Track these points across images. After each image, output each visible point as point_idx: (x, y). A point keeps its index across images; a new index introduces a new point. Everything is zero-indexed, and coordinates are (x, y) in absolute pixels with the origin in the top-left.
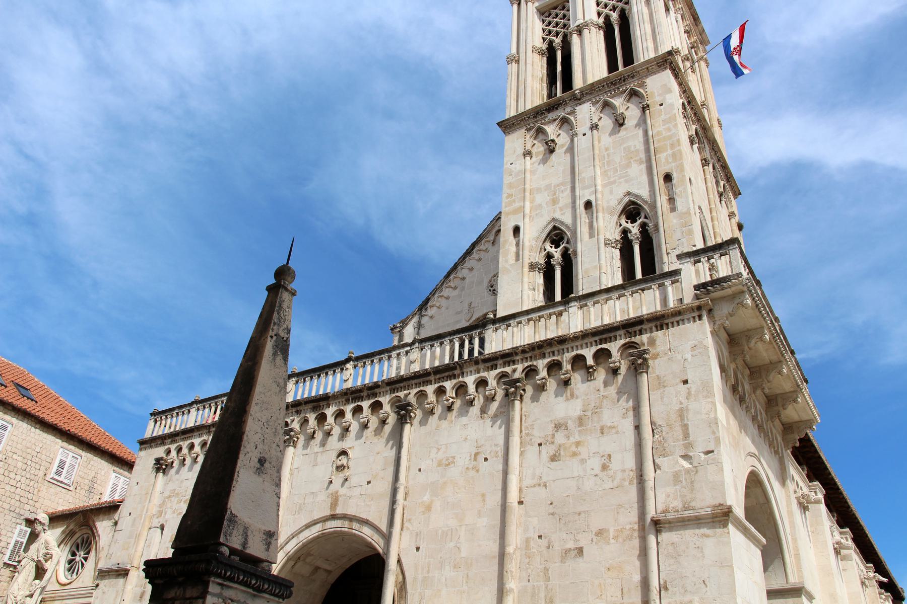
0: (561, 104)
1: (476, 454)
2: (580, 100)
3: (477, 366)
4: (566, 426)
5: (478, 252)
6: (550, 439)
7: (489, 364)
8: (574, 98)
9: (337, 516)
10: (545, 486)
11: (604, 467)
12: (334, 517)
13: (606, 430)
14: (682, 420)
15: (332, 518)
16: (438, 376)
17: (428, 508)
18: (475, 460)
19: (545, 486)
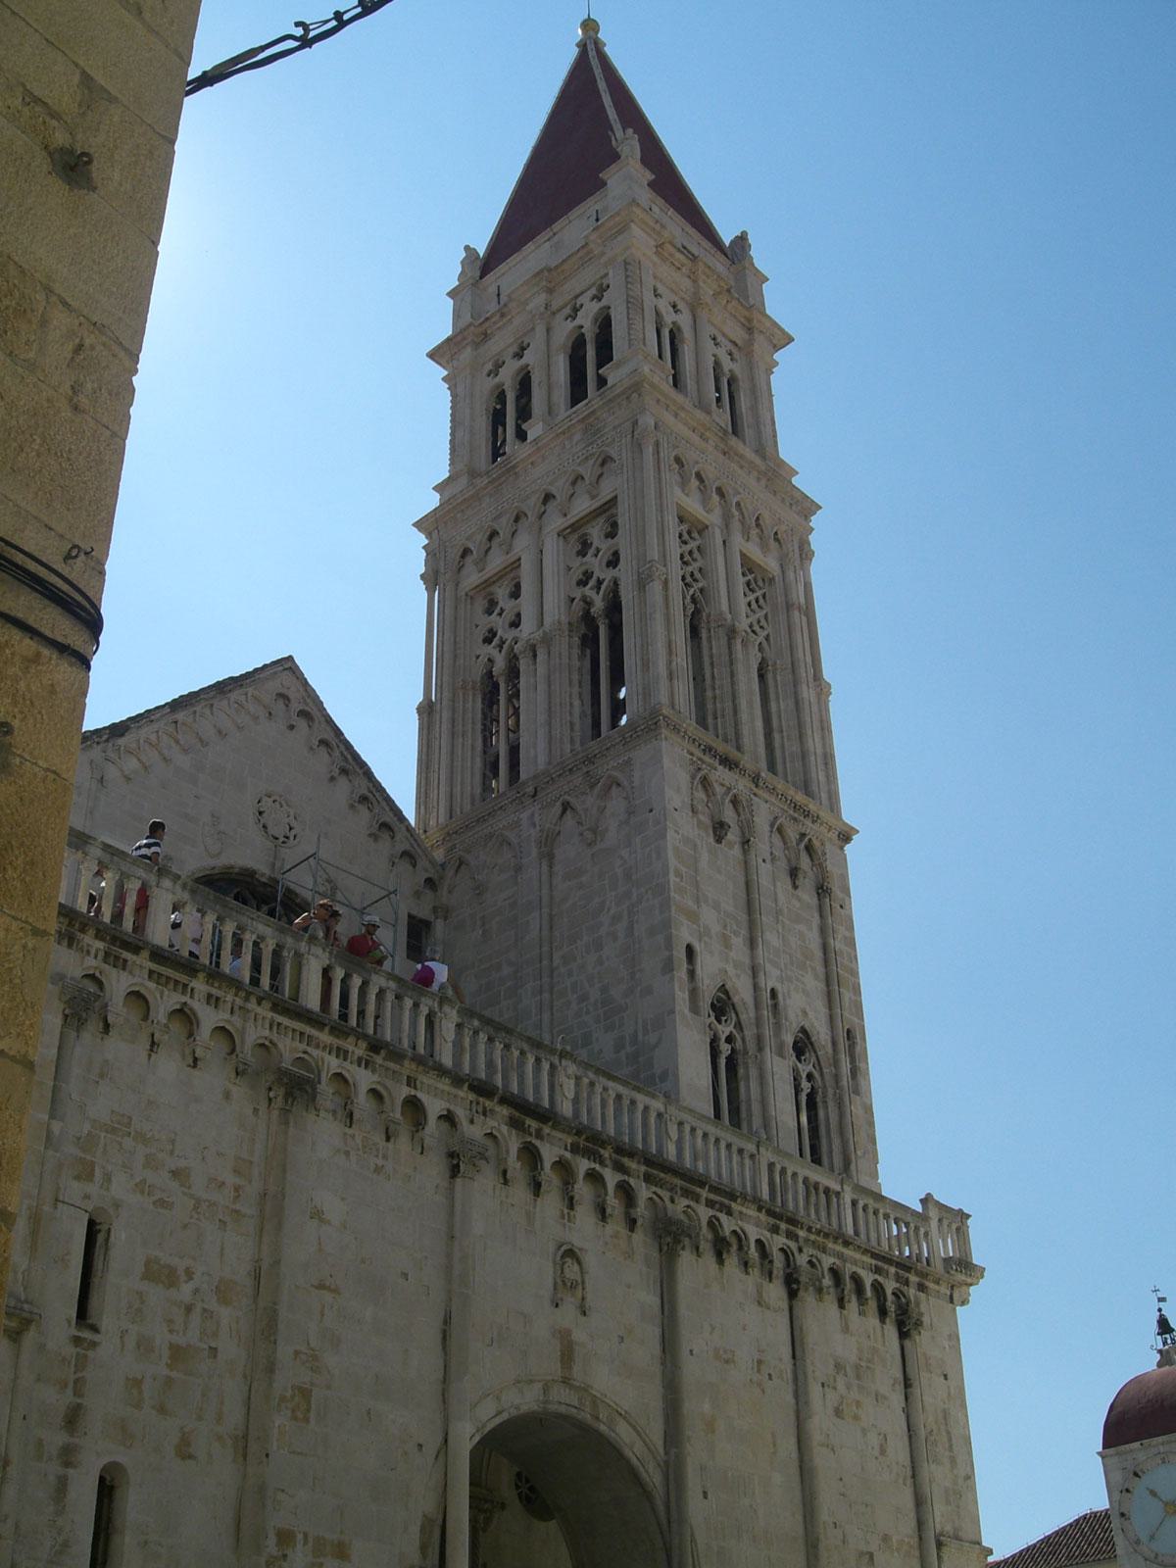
0: (737, 767)
1: (760, 1362)
2: (757, 786)
3: (758, 1214)
4: (845, 1371)
5: (236, 705)
6: (832, 1380)
7: (772, 1221)
8: (754, 778)
9: (571, 1382)
10: (833, 1449)
11: (883, 1451)
12: (566, 1381)
13: (879, 1398)
14: (946, 1425)
15: (564, 1382)
16: (712, 1196)
17: (710, 1426)
18: (759, 1371)
19: (833, 1449)
